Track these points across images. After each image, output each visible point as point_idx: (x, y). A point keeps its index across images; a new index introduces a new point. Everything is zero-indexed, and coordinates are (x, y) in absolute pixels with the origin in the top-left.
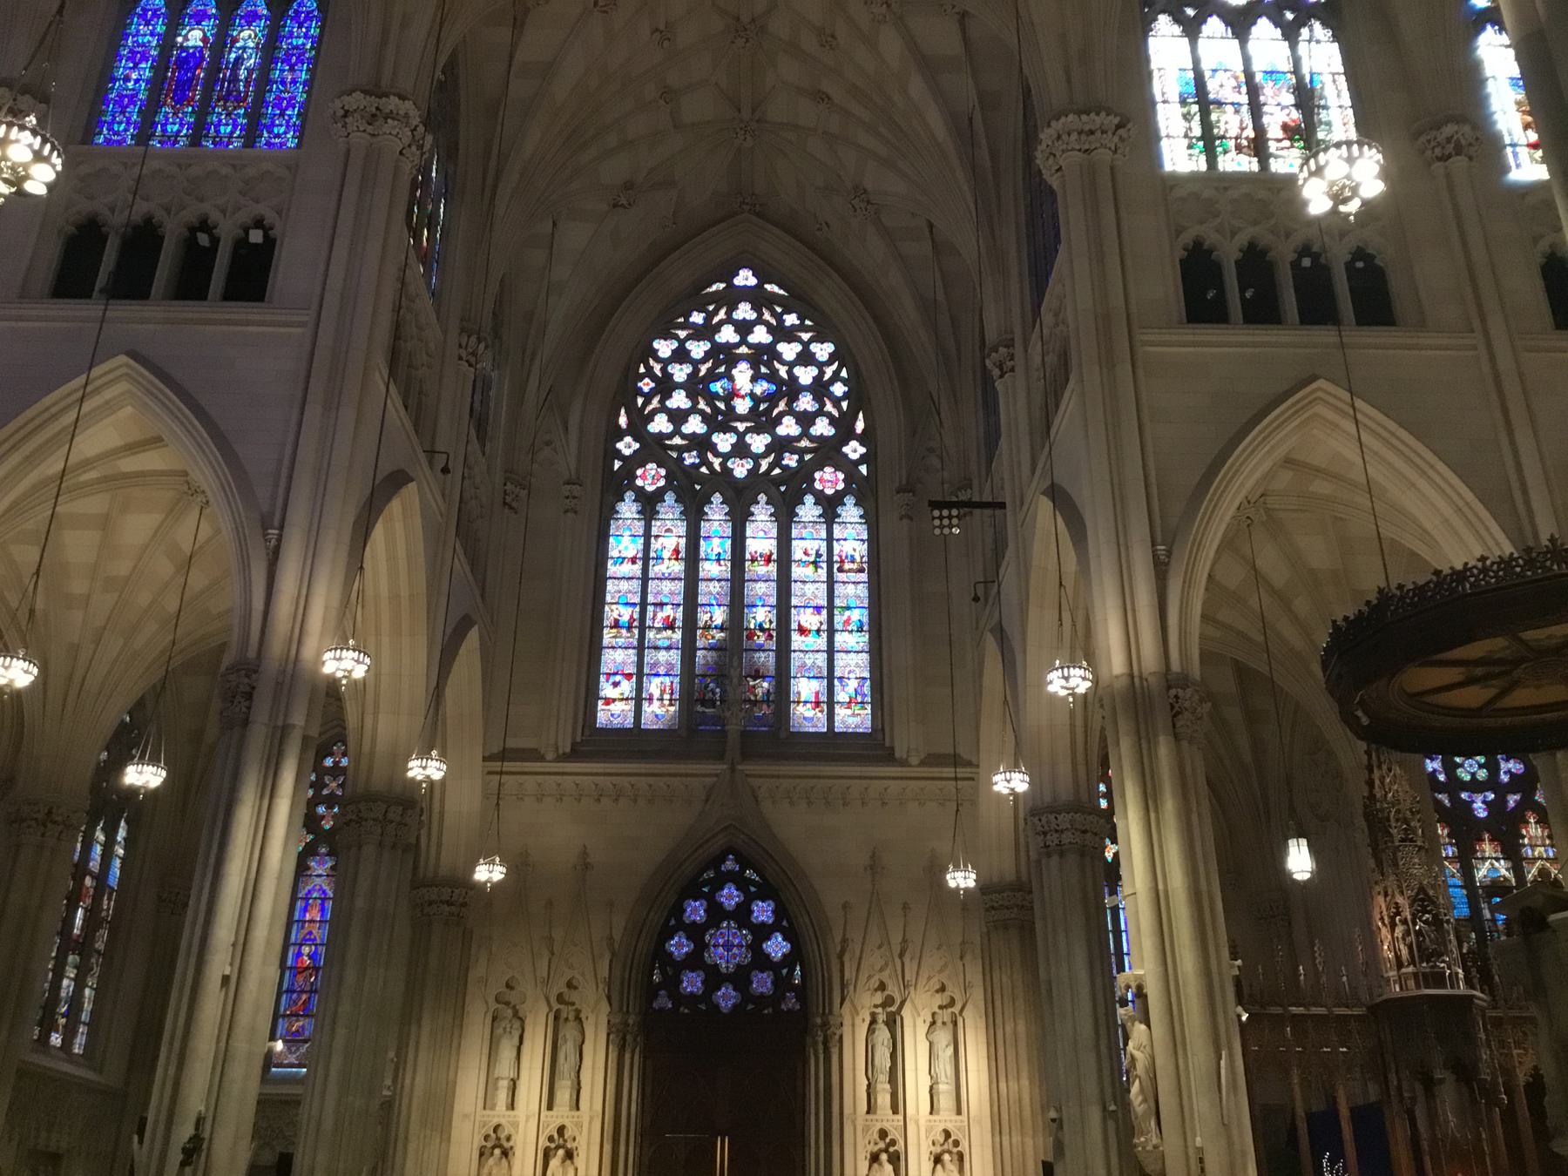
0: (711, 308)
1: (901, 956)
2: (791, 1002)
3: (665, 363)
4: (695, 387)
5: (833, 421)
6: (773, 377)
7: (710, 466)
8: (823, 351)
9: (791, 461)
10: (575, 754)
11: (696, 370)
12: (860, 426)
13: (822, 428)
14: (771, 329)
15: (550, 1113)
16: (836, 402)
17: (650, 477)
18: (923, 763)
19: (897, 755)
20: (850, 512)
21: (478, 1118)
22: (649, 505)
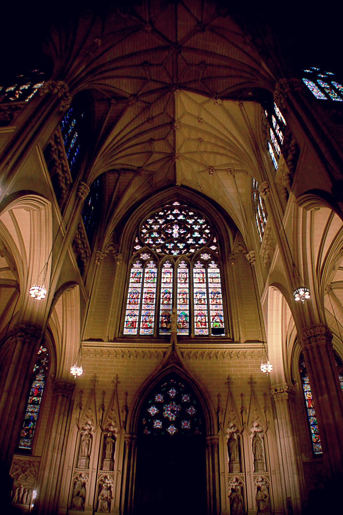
0: (165, 211)
1: (242, 412)
2: (197, 431)
3: (151, 225)
4: (159, 231)
5: (206, 239)
6: (185, 228)
7: (165, 253)
8: (201, 221)
9: (192, 251)
10: (115, 340)
11: (161, 227)
12: (215, 241)
13: (202, 241)
14: (185, 216)
15: (101, 471)
16: (207, 234)
17: (145, 256)
18: (245, 342)
19: (235, 340)
20: (213, 265)
21: (74, 471)
22: (144, 264)
